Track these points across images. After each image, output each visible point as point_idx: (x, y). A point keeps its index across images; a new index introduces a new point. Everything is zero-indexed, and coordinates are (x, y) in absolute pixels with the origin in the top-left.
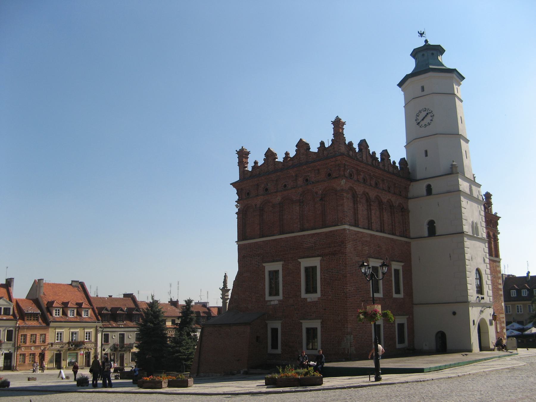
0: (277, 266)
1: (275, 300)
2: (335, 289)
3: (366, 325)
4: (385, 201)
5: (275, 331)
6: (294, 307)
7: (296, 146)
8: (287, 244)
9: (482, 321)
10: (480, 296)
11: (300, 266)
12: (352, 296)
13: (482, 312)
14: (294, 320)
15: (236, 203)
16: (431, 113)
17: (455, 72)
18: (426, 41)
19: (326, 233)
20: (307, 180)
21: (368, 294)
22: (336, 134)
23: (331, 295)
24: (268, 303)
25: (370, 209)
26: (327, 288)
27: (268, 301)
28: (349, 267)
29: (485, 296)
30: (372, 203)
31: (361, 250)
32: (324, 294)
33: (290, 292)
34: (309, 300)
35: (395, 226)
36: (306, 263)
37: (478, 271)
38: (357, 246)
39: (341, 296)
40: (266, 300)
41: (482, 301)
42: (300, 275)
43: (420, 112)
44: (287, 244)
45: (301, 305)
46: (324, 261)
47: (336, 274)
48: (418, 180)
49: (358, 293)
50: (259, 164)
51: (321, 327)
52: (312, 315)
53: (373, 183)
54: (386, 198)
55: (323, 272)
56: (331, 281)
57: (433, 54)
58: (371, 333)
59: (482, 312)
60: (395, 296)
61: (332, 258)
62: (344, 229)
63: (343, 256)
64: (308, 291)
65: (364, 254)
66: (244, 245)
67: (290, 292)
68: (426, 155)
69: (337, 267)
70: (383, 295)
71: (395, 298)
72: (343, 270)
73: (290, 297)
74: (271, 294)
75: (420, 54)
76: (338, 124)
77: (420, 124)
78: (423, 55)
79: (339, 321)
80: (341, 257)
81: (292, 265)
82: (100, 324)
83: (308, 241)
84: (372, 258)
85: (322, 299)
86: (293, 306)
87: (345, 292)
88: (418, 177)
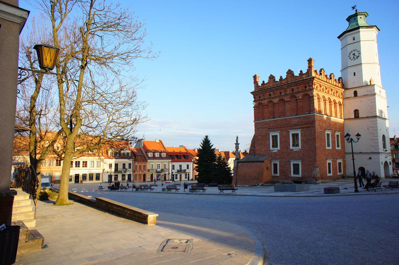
0: (277, 134)
1: (275, 150)
4: (332, 100)
5: (275, 165)
7: (287, 73)
9: (386, 162)
10: (385, 149)
15: (253, 102)
17: (375, 27)
18: (356, 11)
19: (304, 117)
20: (293, 90)
24: (272, 151)
25: (326, 104)
34: (294, 150)
36: (292, 132)
37: (384, 136)
41: (386, 152)
43: (352, 52)
48: (349, 89)
50: (265, 83)
58: (327, 167)
60: (337, 148)
62: (314, 115)
66: (258, 123)
68: (355, 75)
71: (337, 150)
74: (273, 147)
75: (352, 19)
76: (310, 61)
77: (351, 59)
82: (171, 160)
84: (327, 129)
88: (349, 87)
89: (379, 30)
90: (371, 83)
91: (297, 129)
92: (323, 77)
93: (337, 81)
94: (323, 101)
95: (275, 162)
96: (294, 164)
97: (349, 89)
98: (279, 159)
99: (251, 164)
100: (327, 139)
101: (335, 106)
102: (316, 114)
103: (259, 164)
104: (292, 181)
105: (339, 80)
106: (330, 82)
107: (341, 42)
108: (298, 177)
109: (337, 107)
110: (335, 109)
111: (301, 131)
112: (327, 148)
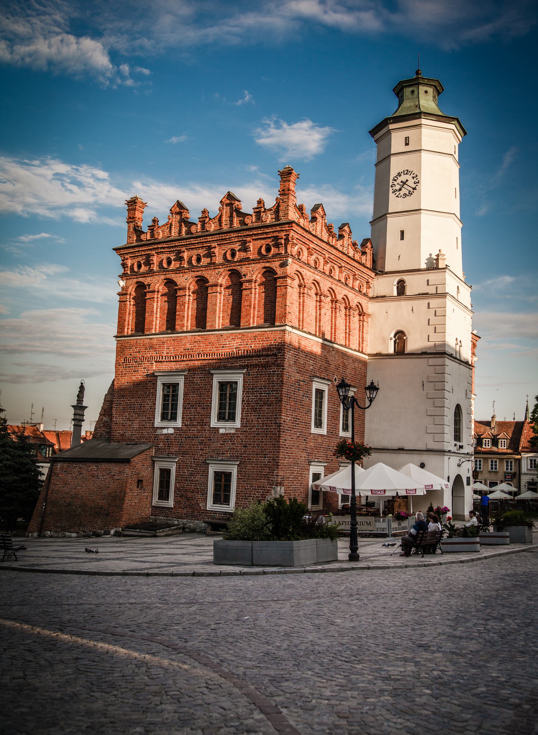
2: (263, 418)
3: (301, 474)
4: (339, 297)
5: (165, 473)
6: (198, 440)
8: (194, 346)
9: (458, 478)
11: (212, 380)
12: (287, 430)
13: (459, 465)
14: (196, 459)
16: (415, 178)
21: (308, 428)
22: (283, 190)
23: (255, 426)
24: (159, 432)
26: (251, 416)
27: (157, 428)
28: (286, 387)
29: (464, 443)
30: (322, 298)
31: (303, 364)
32: (246, 424)
33: (194, 418)
35: (349, 335)
38: (299, 358)
39: (271, 429)
40: (155, 426)
41: (462, 451)
42: (211, 394)
44: (194, 346)
45: (210, 437)
46: (249, 375)
47: (266, 396)
48: (387, 273)
49: (295, 426)
51: (238, 471)
52: (225, 454)
53: (327, 268)
54: (341, 292)
55: (247, 392)
56: (257, 406)
57: (426, 92)
59: (459, 465)
61: (262, 372)
62: (284, 331)
63: (278, 371)
64: (221, 417)
65: (307, 370)
67: (194, 418)
68: (402, 238)
69: (269, 386)
70: (328, 432)
72: (277, 391)
73: (193, 425)
74: (164, 417)
78: (413, 92)
79: (266, 465)
80: (275, 371)
81: (200, 378)
83: (226, 344)
84: (317, 377)
85: (242, 431)
86: (197, 437)
87: (277, 423)
89: (465, 133)
90: (437, 264)
91: (235, 368)
92: (319, 228)
93: (359, 247)
94: (314, 296)
95: (165, 465)
96: (217, 474)
97: (387, 273)
98: (177, 454)
99: (94, 467)
100: (316, 406)
101: (346, 315)
102: (288, 328)
103: (115, 468)
104: (205, 522)
105: (363, 245)
106: (338, 246)
107: (379, 148)
108: (225, 513)
109: (351, 317)
110: (346, 323)
111: (244, 374)
112: (314, 430)
